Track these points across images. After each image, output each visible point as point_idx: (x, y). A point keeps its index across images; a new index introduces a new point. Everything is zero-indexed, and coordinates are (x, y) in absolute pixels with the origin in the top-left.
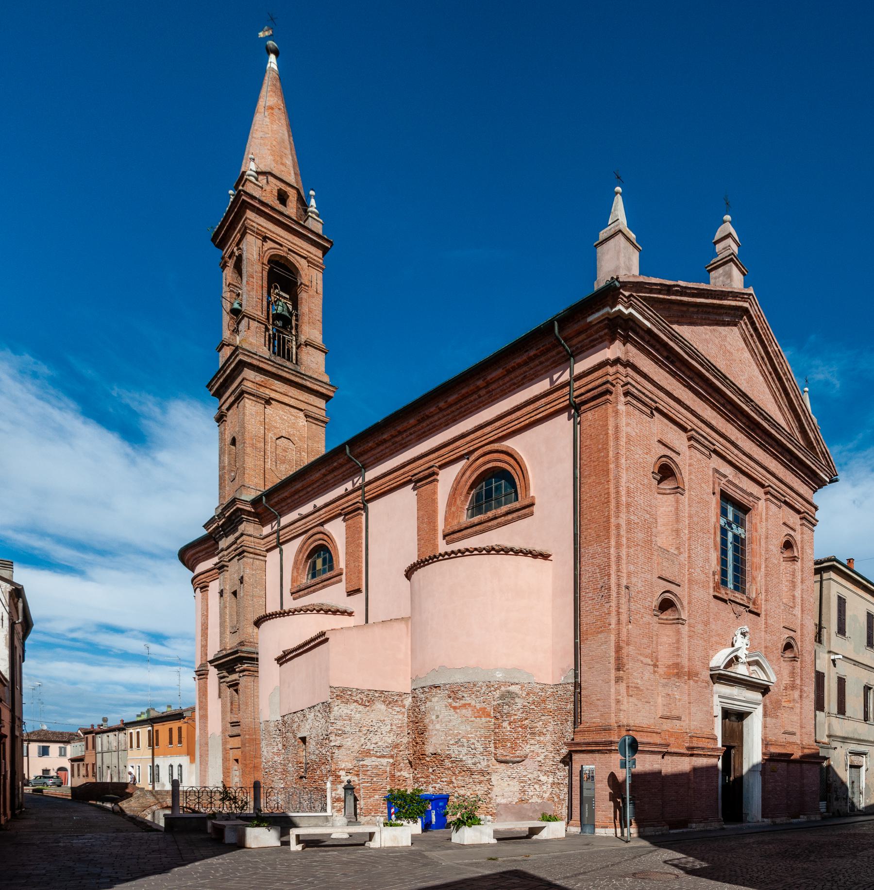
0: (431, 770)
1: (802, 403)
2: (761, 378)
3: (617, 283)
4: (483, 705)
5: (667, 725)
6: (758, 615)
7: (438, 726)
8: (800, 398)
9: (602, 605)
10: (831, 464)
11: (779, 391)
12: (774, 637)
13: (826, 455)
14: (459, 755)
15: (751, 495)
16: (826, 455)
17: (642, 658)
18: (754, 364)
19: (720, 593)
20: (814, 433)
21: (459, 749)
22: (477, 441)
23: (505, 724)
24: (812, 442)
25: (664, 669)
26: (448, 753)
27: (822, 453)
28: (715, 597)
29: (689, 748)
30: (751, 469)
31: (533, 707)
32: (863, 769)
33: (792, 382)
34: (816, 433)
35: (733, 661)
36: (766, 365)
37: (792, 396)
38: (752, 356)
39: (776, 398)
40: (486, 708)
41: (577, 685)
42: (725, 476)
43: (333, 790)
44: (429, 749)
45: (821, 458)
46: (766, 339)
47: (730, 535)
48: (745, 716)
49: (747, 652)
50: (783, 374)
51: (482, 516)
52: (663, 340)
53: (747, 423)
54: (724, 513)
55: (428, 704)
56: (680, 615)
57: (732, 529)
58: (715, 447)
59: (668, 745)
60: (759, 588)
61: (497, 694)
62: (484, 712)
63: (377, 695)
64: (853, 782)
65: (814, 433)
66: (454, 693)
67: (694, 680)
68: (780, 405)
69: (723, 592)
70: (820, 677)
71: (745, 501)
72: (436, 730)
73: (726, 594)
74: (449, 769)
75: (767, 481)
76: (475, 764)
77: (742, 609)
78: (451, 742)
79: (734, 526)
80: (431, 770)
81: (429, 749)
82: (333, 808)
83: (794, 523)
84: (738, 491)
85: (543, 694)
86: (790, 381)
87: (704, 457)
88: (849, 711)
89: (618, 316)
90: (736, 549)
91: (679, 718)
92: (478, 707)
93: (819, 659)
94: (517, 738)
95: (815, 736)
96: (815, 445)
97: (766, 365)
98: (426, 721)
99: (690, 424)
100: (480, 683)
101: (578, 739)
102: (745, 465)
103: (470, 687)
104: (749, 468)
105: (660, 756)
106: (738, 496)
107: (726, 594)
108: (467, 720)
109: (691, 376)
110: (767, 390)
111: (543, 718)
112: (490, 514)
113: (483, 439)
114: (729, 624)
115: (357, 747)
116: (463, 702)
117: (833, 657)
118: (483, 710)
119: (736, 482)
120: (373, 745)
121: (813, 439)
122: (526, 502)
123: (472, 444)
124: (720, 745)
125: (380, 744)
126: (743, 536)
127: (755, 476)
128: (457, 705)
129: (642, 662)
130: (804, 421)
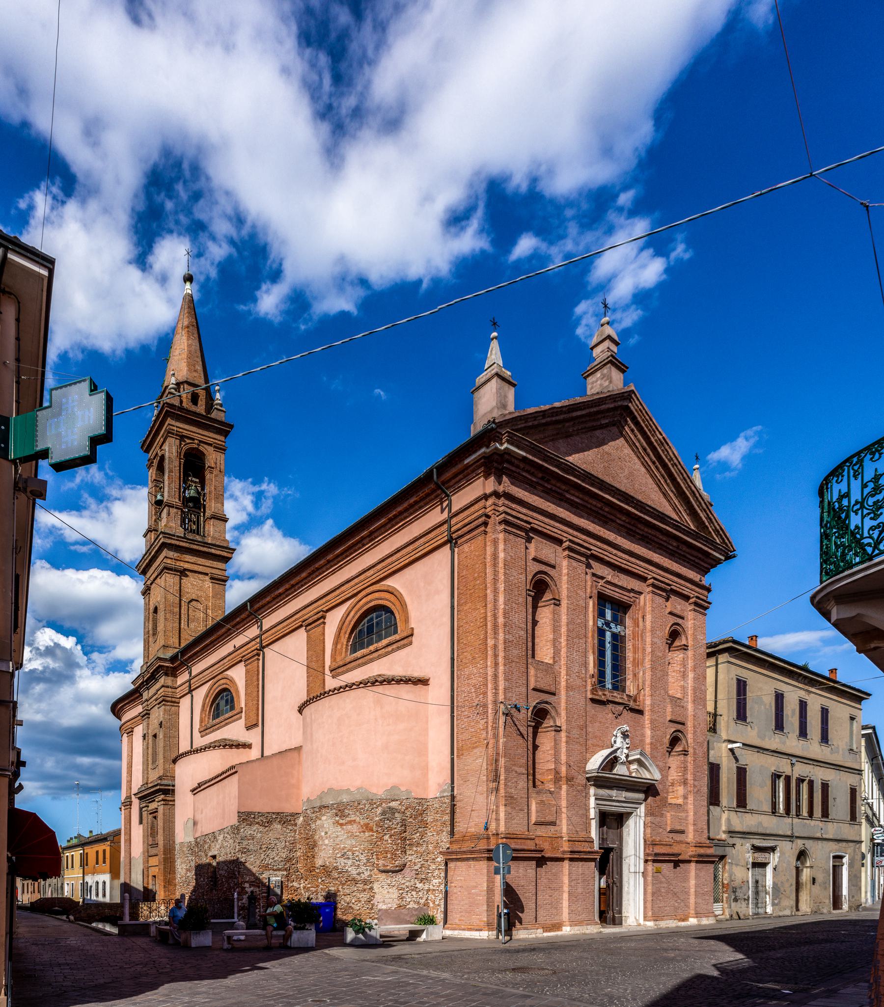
0: (320, 880)
1: (691, 484)
2: (643, 469)
3: (494, 426)
4: (366, 821)
5: (541, 831)
7: (326, 842)
8: (688, 480)
9: (478, 722)
10: (726, 541)
11: (664, 478)
13: (721, 532)
14: (345, 866)
15: (632, 591)
16: (721, 532)
17: (517, 769)
18: (635, 458)
19: (598, 695)
20: (705, 511)
21: (345, 861)
22: (360, 584)
23: (387, 837)
24: (703, 523)
26: (335, 865)
27: (716, 531)
30: (632, 565)
32: (769, 870)
33: (679, 466)
34: (708, 512)
35: (611, 762)
36: (648, 455)
37: (679, 480)
38: (633, 450)
39: (661, 486)
40: (369, 824)
41: (453, 797)
42: (602, 578)
43: (239, 900)
44: (319, 862)
45: (715, 536)
46: (649, 430)
47: (608, 635)
48: (624, 819)
50: (669, 460)
51: (364, 650)
52: (538, 464)
53: (627, 521)
54: (602, 614)
55: (318, 822)
56: (555, 722)
57: (611, 628)
58: (592, 552)
59: (542, 851)
60: (641, 684)
61: (379, 810)
62: (367, 828)
63: (274, 817)
64: (757, 882)
65: (705, 511)
66: (340, 811)
68: (665, 492)
69: (600, 693)
70: (714, 770)
71: (625, 597)
72: (325, 845)
73: (604, 695)
74: (337, 879)
75: (650, 573)
76: (359, 874)
77: (621, 708)
78: (338, 856)
79: (612, 625)
80: (320, 880)
81: (319, 862)
82: (239, 915)
83: (682, 610)
84: (617, 590)
86: (676, 466)
87: (580, 564)
88: (751, 804)
89: (495, 453)
90: (615, 648)
92: (362, 823)
94: (397, 850)
95: (709, 832)
96: (707, 524)
97: (648, 455)
98: (316, 837)
99: (565, 535)
100: (364, 802)
101: (455, 847)
102: (625, 562)
103: (356, 805)
104: (629, 564)
106: (616, 594)
107: (604, 695)
108: (352, 836)
109: (567, 489)
110: (650, 481)
112: (372, 648)
113: (365, 582)
114: (607, 725)
115: (258, 863)
116: (348, 819)
117: (730, 746)
118: (367, 825)
119: (616, 581)
120: (271, 860)
121: (704, 519)
122: (405, 634)
123: (356, 587)
124: (596, 847)
125: (276, 858)
126: (623, 634)
127: (636, 571)
128: (343, 822)
129: (516, 772)
130: (693, 502)
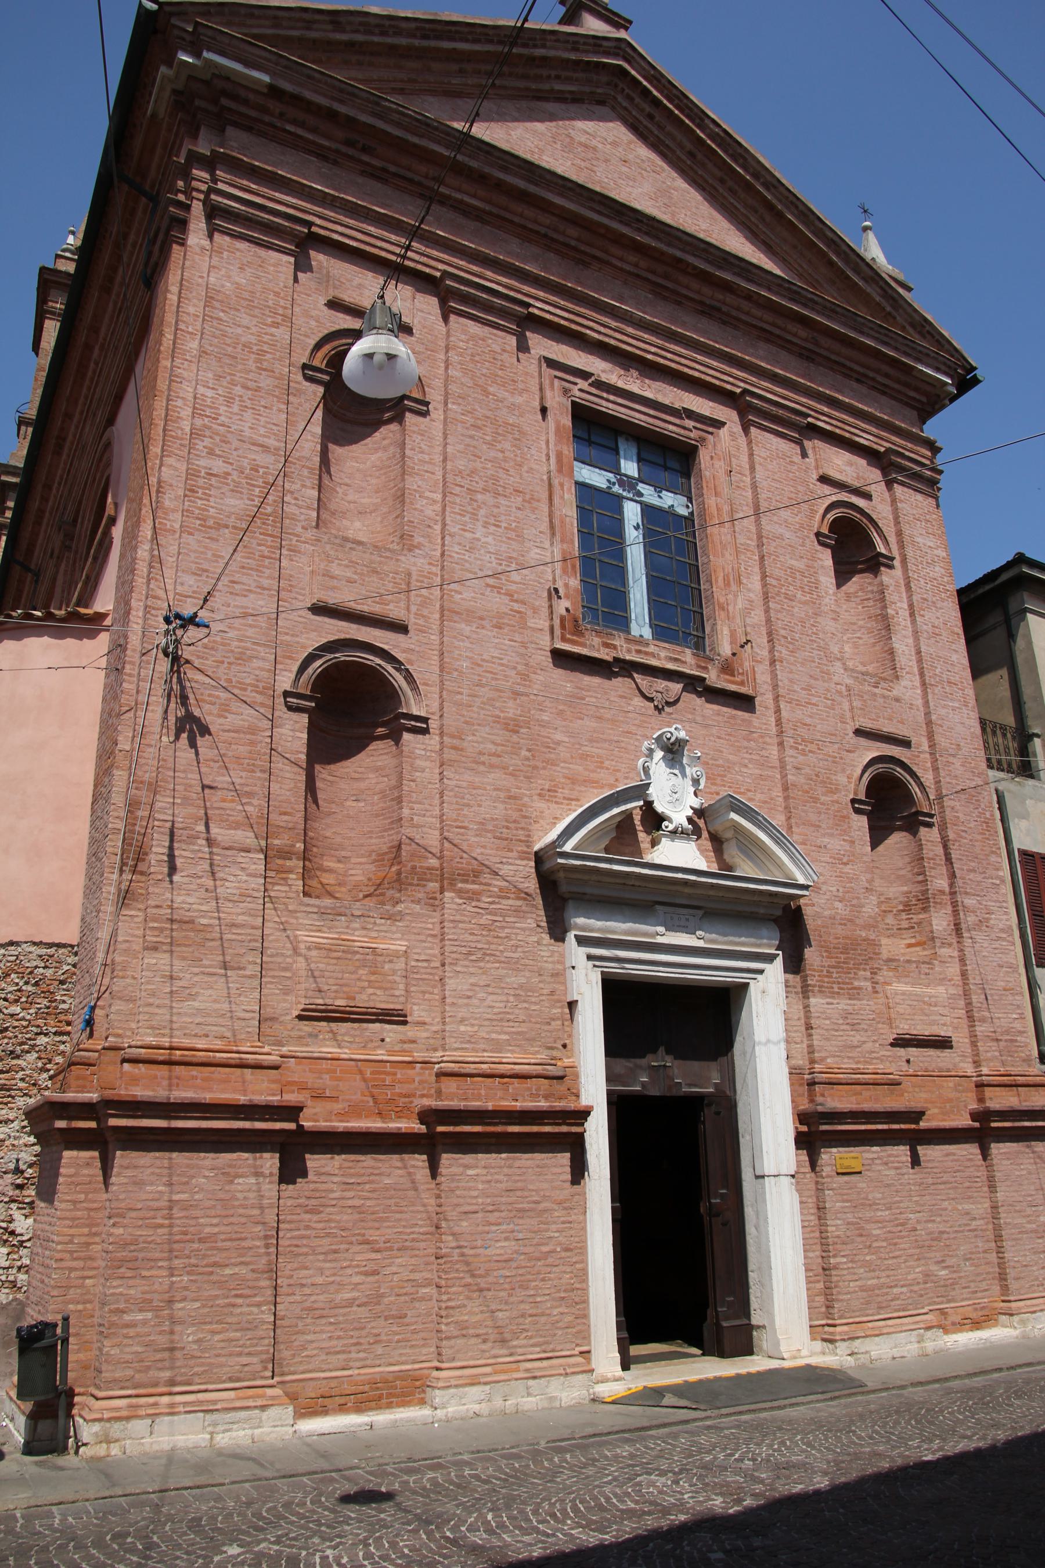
6: (745, 702)
12: (812, 758)
25: (371, 866)
28: (561, 658)
29: (428, 1116)
31: (16, 1009)
49: (696, 803)
67: (460, 892)
85: (49, 973)
91: (395, 1017)
93: (1025, 816)
105: (270, 1162)
111: (42, 1040)
